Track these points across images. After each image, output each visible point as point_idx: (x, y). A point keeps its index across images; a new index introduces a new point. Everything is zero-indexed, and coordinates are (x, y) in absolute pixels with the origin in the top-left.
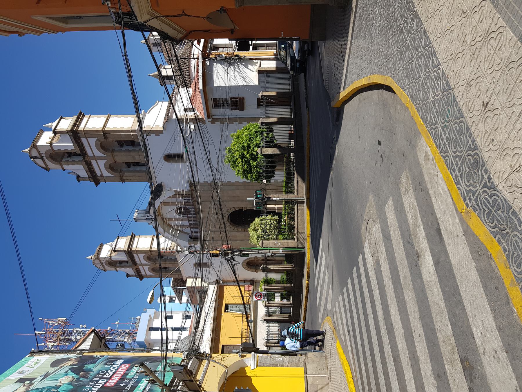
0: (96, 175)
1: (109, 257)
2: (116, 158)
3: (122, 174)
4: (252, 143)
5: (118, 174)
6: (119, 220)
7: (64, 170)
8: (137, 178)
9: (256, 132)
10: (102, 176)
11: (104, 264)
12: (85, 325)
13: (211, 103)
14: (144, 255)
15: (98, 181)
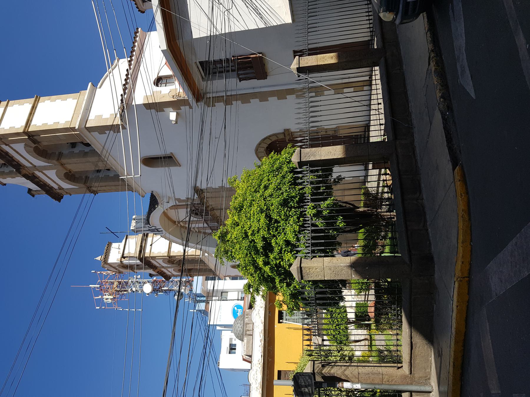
0: (52, 188)
1: (119, 262)
2: (69, 167)
3: (88, 184)
4: (274, 236)
5: (82, 185)
6: (113, 233)
7: (5, 185)
8: (113, 188)
9: (285, 203)
10: (60, 188)
11: (117, 268)
12: (139, 276)
13: (196, 74)
14: (162, 260)
15: (59, 195)
